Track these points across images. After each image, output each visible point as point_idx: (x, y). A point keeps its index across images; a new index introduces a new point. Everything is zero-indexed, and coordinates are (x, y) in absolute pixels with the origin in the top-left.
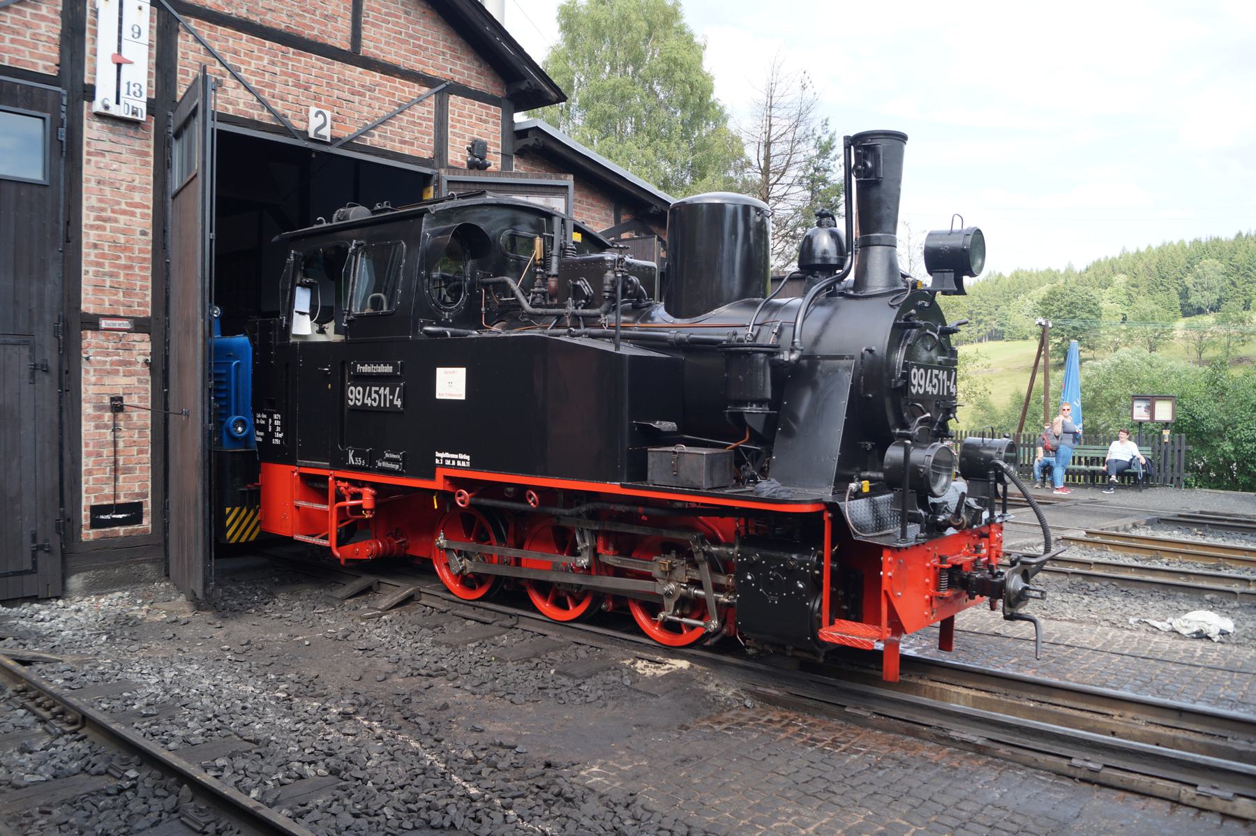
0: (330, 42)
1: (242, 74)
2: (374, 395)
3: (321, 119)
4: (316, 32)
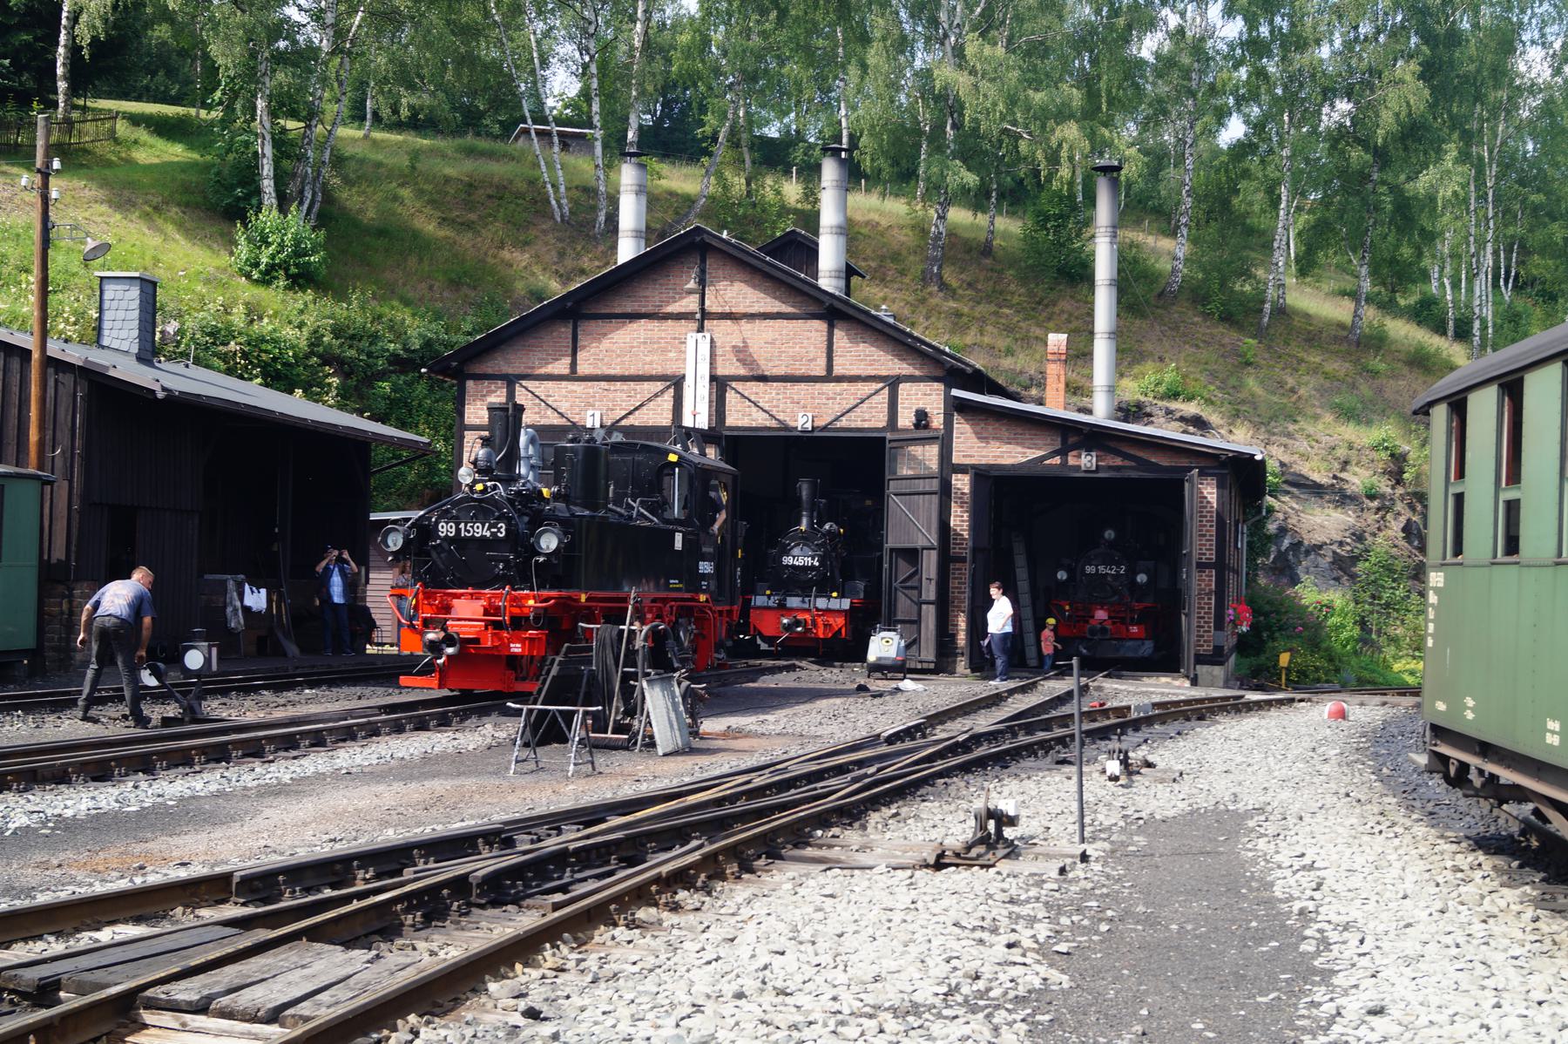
0: (813, 374)
3: (805, 418)
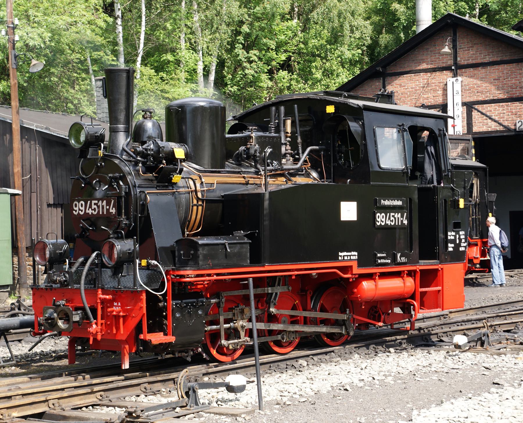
1: (493, 117)
2: (392, 218)
4: (518, 94)
